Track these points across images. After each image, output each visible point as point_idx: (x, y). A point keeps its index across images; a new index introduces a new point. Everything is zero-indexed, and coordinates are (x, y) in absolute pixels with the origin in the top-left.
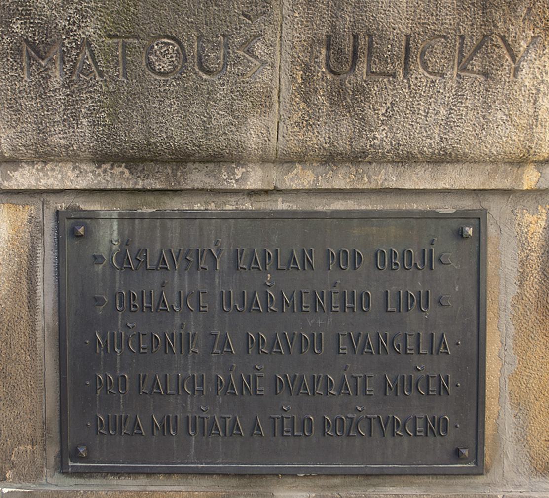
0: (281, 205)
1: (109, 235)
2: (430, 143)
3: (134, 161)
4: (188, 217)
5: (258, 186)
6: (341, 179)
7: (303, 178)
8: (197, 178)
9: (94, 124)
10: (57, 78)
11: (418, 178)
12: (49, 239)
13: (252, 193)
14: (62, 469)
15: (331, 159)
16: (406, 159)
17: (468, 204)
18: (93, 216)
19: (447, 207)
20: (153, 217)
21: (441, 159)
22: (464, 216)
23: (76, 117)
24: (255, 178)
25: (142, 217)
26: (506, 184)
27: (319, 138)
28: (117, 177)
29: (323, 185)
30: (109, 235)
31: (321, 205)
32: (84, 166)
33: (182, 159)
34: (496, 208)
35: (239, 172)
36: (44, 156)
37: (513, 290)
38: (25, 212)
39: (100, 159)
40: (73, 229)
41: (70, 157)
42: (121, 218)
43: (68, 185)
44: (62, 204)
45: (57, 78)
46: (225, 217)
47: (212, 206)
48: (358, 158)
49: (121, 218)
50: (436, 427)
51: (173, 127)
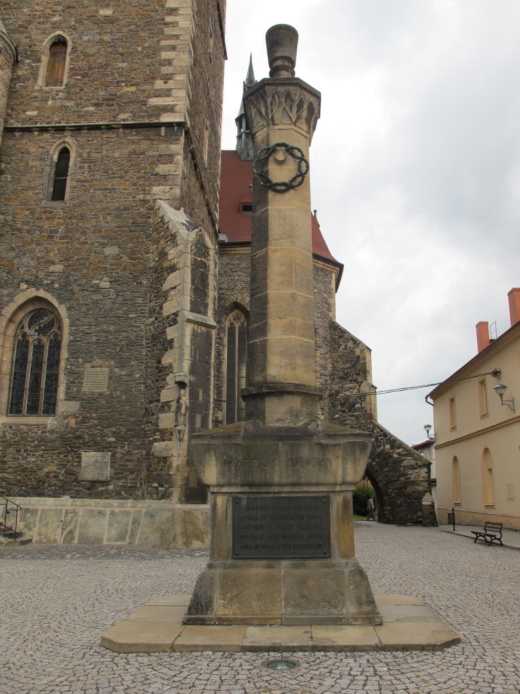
0: (283, 495)
1: (244, 503)
2: (314, 481)
3: (250, 485)
4: (262, 498)
5: (278, 491)
6: (296, 489)
7: (287, 489)
8: (264, 489)
9: (241, 478)
10: (233, 468)
11: (313, 489)
12: (231, 504)
13: (277, 492)
14: (234, 559)
15: (293, 485)
16: (310, 485)
17: (324, 494)
18: (240, 498)
19: (320, 495)
20: (254, 498)
21: (317, 484)
22: (324, 497)
23: (237, 476)
24: (276, 489)
25: (252, 498)
26: (333, 490)
27: (290, 481)
28: (247, 489)
29: (292, 491)
30: (244, 503)
31: (291, 495)
32: (239, 487)
33: (260, 485)
34: (332, 495)
35: (273, 488)
36: (229, 485)
37: (336, 514)
38: (226, 497)
39: (242, 485)
40: (236, 501)
41: (235, 485)
42: (247, 499)
43: (235, 491)
44: (234, 495)
45: (233, 468)
46: (270, 498)
47: (268, 496)
48: (299, 484)
49: (247, 499)
50: (319, 546)
51: (257, 478)
